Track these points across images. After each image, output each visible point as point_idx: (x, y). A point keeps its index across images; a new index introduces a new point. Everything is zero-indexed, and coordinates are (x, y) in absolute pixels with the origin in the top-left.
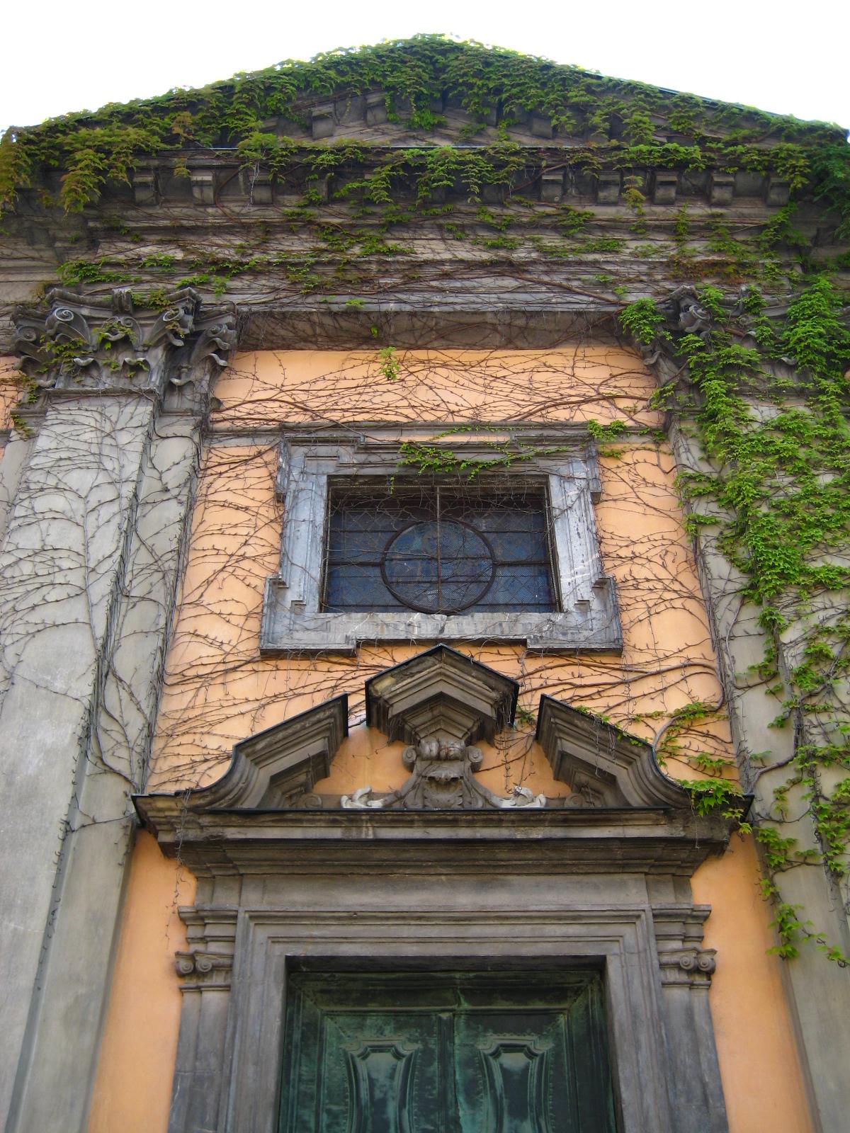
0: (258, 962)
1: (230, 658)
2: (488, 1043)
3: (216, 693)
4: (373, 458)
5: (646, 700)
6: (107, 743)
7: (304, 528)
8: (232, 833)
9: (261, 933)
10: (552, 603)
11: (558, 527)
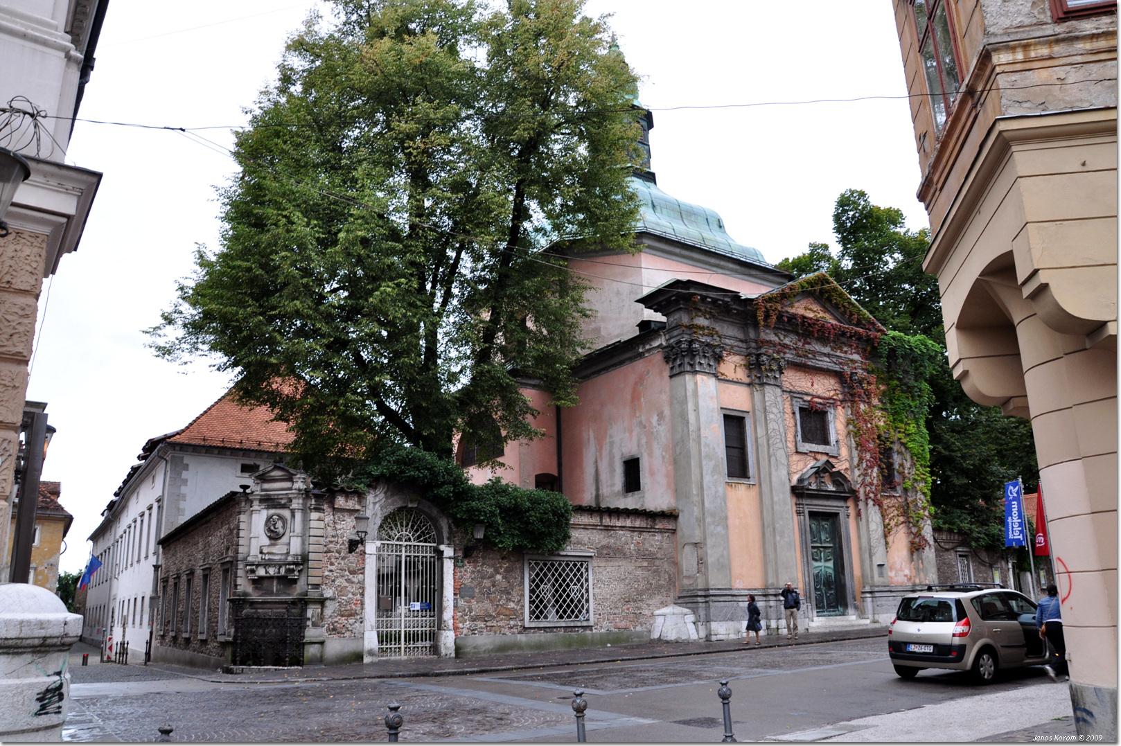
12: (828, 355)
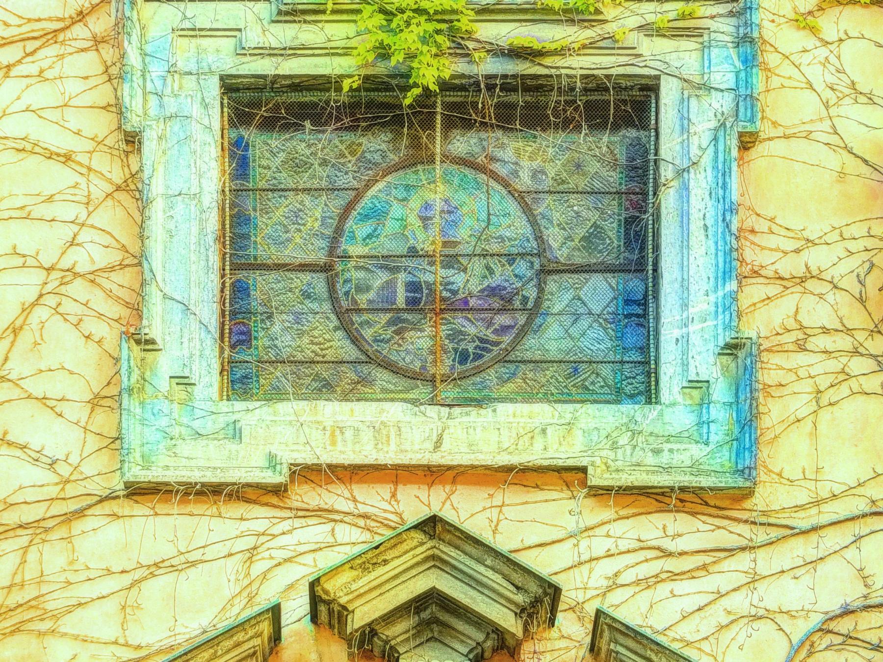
1: (71, 490)
3: (52, 557)
5: (786, 578)
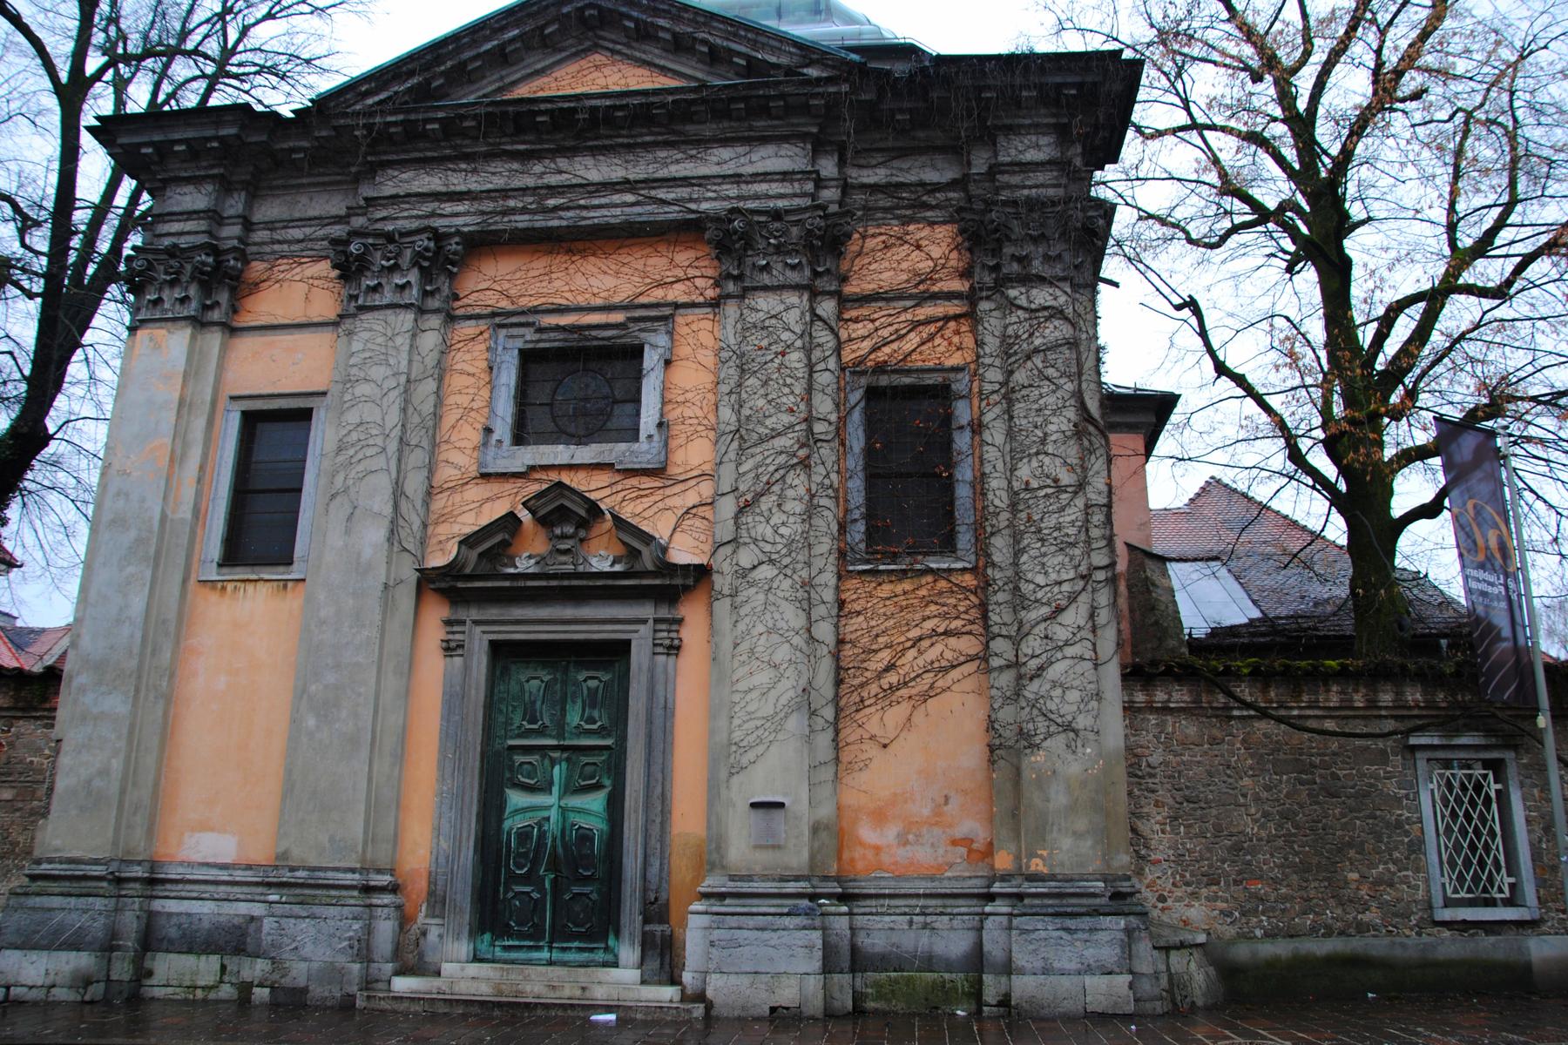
0: (477, 643)
2: (581, 677)
3: (457, 498)
4: (544, 336)
6: (403, 534)
7: (503, 389)
8: (460, 585)
9: (479, 629)
10: (633, 434)
11: (644, 382)
12: (627, 185)
